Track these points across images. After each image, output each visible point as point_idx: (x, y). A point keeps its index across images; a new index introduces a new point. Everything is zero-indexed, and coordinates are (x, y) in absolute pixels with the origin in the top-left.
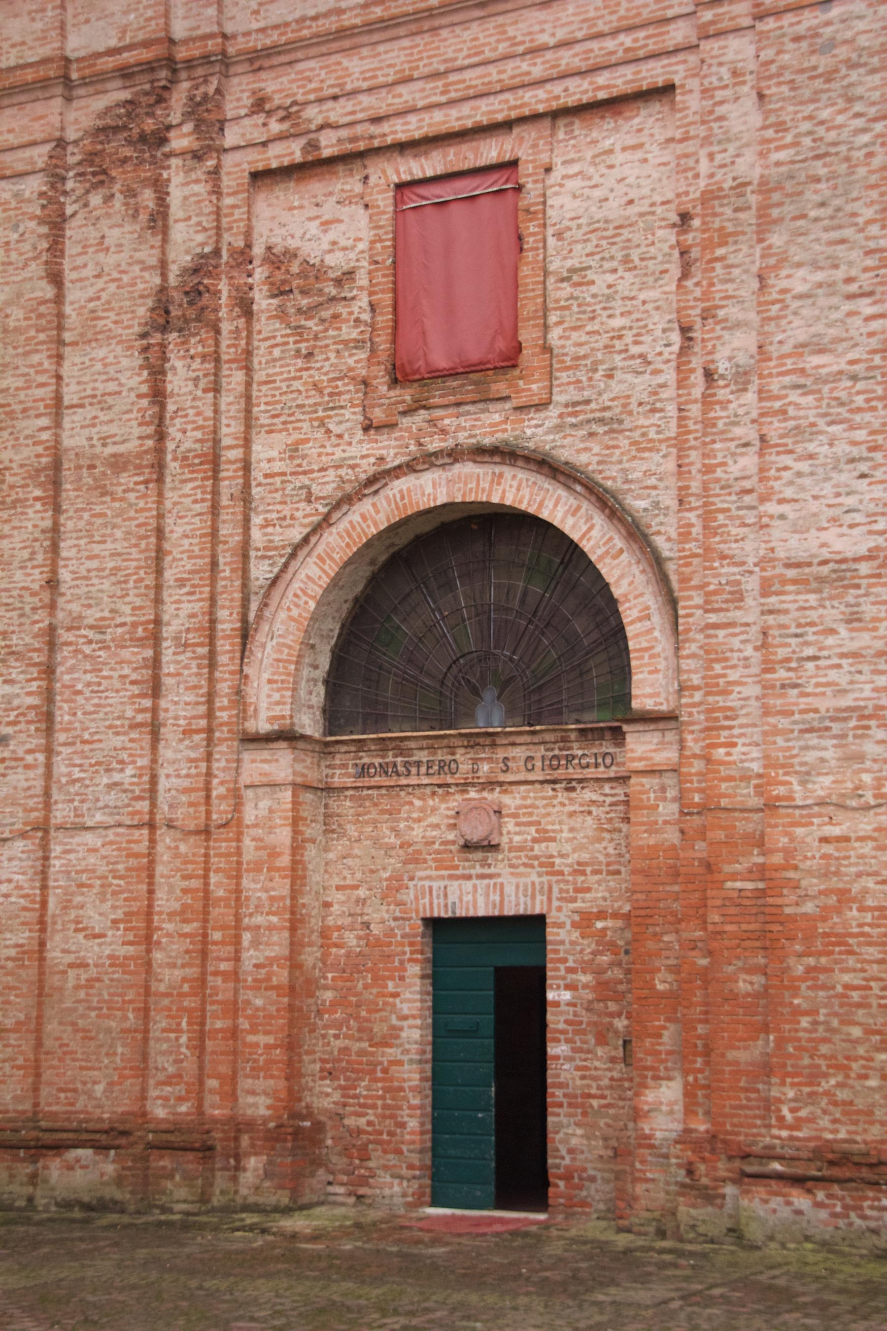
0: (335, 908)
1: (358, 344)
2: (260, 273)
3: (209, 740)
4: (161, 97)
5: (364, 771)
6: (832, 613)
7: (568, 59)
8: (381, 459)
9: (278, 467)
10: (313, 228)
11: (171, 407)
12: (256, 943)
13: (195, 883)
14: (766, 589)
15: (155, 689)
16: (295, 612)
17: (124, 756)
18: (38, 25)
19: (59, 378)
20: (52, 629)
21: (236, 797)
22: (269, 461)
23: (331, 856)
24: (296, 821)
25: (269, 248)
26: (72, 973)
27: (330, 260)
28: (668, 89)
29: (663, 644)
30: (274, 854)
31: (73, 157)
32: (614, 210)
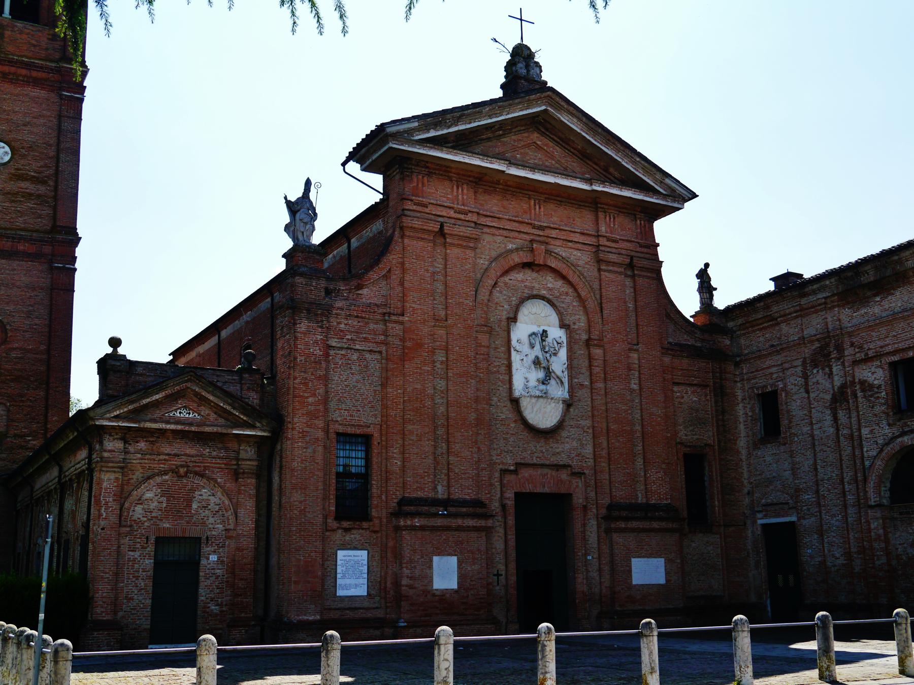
0: (899, 550)
1: (884, 404)
2: (858, 387)
3: (860, 508)
4: (827, 345)
5: (901, 514)
8: (893, 433)
9: (868, 436)
10: (870, 374)
11: (839, 422)
12: (878, 559)
13: (860, 545)
15: (844, 495)
16: (877, 474)
17: (839, 513)
18: (797, 330)
19: (811, 417)
20: (817, 481)
21: (868, 522)
22: (866, 434)
23: (897, 536)
24: (884, 528)
25: (859, 380)
26: (833, 568)
27: (875, 383)
30: (879, 536)
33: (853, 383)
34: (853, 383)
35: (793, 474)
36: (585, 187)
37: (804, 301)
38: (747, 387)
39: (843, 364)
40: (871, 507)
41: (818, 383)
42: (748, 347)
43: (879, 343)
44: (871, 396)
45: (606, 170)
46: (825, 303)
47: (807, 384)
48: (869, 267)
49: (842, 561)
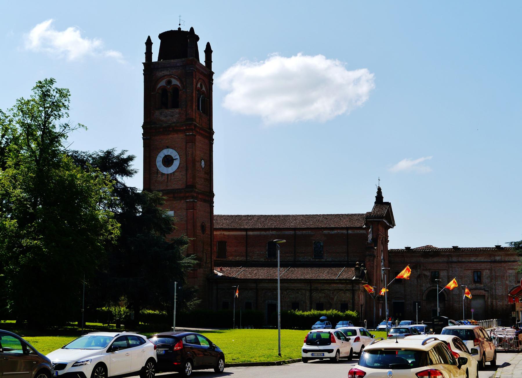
2: (423, 275)
28: (447, 270)
36: (389, 225)
39: (420, 270)
40: (424, 300)
41: (414, 272)
43: (430, 267)
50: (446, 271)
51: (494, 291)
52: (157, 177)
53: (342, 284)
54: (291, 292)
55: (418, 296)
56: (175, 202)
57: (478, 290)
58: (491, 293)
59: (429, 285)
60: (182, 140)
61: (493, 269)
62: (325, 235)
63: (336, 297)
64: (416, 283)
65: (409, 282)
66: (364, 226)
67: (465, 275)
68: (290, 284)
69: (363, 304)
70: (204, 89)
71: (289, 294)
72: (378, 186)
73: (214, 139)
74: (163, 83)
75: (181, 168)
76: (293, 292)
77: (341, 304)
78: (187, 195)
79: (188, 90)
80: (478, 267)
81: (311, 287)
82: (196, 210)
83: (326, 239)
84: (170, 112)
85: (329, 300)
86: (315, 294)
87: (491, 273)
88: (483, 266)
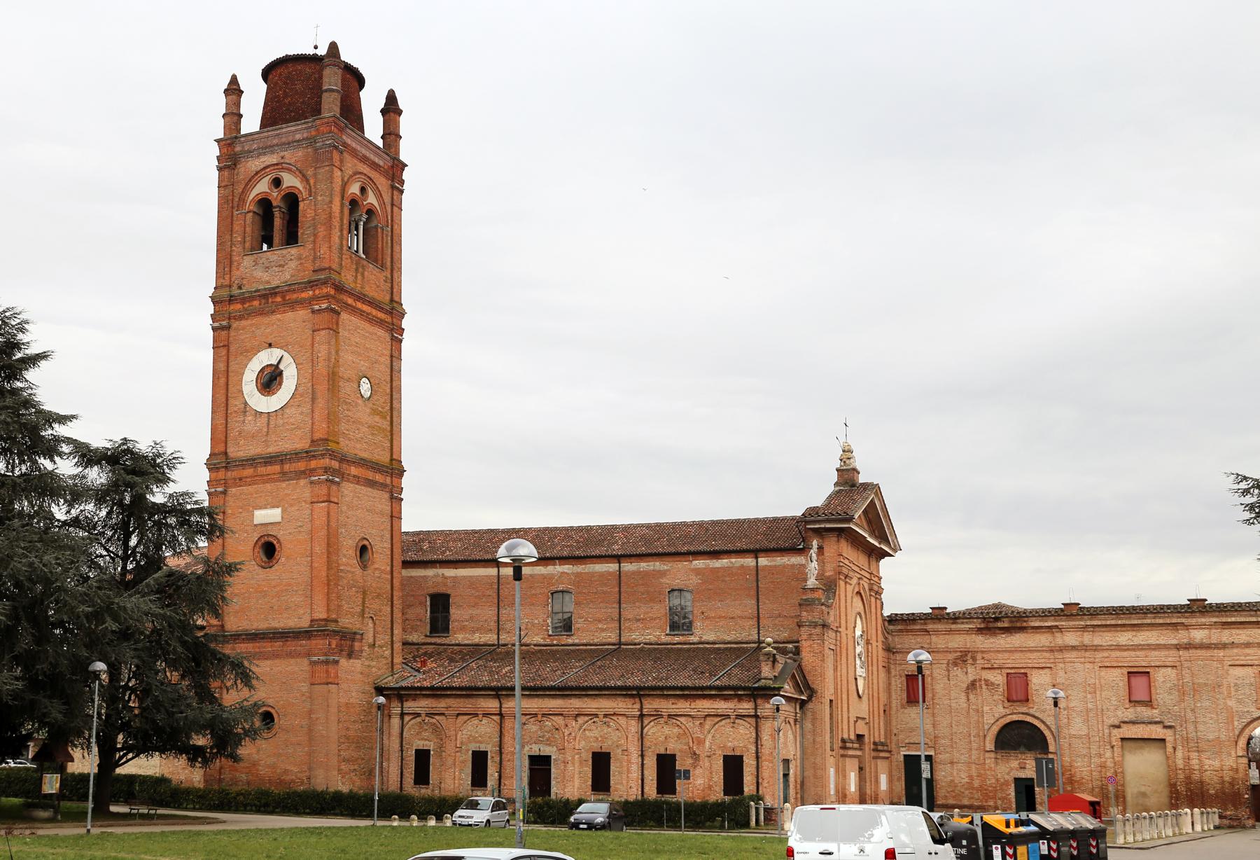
2: (983, 682)
4: (966, 655)
5: (1002, 756)
6: (1080, 742)
7: (1035, 661)
10: (992, 677)
14: (1070, 738)
21: (985, 759)
28: (1051, 668)
29: (1053, 743)
31: (951, 662)
32: (1043, 682)
33: (980, 680)
34: (980, 680)
35: (934, 727)
37: (953, 626)
38: (898, 669)
42: (901, 644)
44: (993, 689)
45: (874, 531)
46: (968, 631)
47: (949, 675)
48: (1007, 619)
49: (967, 780)
50: (1047, 671)
51: (1191, 728)
52: (244, 421)
53: (726, 698)
54: (590, 722)
55: (972, 738)
56: (284, 485)
57: (1144, 725)
58: (1185, 733)
59: (1000, 710)
60: (304, 324)
61: (1186, 664)
62: (697, 572)
63: (710, 736)
64: (965, 705)
65: (946, 702)
66: (799, 545)
67: (1102, 681)
68: (586, 699)
69: (791, 757)
70: (372, 199)
71: (584, 727)
72: (842, 439)
73: (403, 330)
74: (263, 187)
75: (302, 395)
76: (594, 722)
77: (725, 757)
78: (313, 464)
79: (319, 198)
80: (1140, 659)
81: (641, 709)
82: (338, 504)
83: (700, 581)
84: (275, 258)
85: (691, 745)
86: (652, 729)
87: (1180, 677)
88: (1155, 657)
